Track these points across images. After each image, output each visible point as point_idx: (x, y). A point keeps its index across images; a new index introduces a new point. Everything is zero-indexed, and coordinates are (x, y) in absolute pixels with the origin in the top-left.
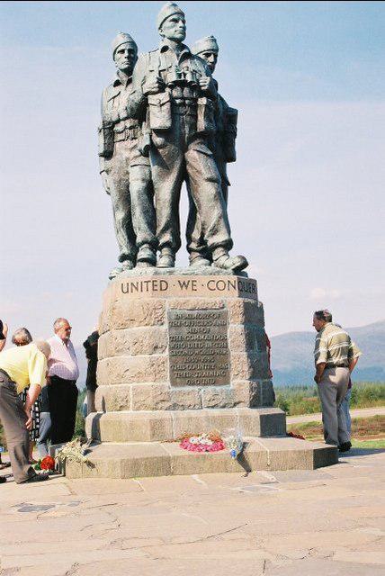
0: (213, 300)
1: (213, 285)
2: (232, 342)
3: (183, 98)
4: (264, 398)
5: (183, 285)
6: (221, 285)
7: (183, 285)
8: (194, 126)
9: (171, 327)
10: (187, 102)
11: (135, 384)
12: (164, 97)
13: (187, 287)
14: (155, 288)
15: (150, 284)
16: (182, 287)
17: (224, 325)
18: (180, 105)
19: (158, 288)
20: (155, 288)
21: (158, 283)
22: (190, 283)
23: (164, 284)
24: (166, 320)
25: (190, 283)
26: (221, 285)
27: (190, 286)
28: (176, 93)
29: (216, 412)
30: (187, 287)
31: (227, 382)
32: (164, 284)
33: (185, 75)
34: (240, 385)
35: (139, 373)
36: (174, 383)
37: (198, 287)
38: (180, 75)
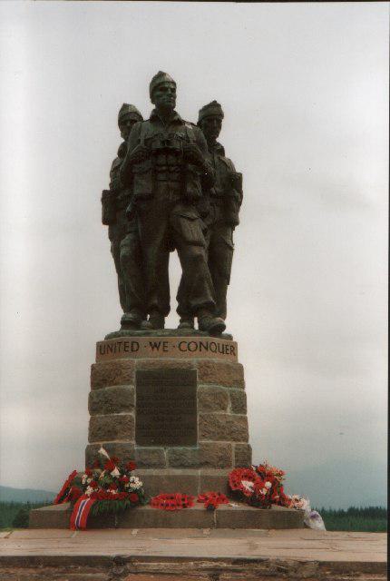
0: (181, 360)
1: (184, 346)
2: (200, 401)
3: (167, 165)
4: (237, 461)
5: (155, 346)
6: (192, 346)
8: (182, 190)
10: (173, 169)
11: (105, 442)
12: (146, 165)
15: (122, 346)
17: (194, 384)
18: (163, 172)
19: (130, 349)
21: (130, 345)
22: (162, 344)
23: (135, 346)
24: (134, 380)
25: (162, 344)
26: (192, 346)
27: (161, 347)
28: (162, 160)
29: (178, 472)
31: (194, 443)
33: (169, 142)
34: (207, 445)
35: (109, 431)
36: (139, 443)
37: (169, 348)
38: (163, 142)
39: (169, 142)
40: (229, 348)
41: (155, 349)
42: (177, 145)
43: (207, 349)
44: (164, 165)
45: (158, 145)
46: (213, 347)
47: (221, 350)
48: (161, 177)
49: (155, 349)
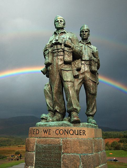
1: (57, 132)
3: (58, 49)
5: (45, 132)
6: (61, 132)
7: (45, 132)
9: (36, 153)
10: (59, 51)
13: (46, 133)
14: (34, 133)
16: (44, 133)
18: (55, 52)
19: (35, 133)
20: (34, 133)
22: (48, 130)
23: (38, 131)
25: (48, 130)
26: (61, 132)
28: (55, 47)
30: (46, 133)
32: (37, 131)
39: (57, 40)
40: (82, 131)
41: (45, 133)
42: (60, 41)
43: (68, 133)
44: (56, 50)
45: (54, 42)
46: (71, 132)
47: (76, 133)
48: (55, 55)
49: (45, 133)
